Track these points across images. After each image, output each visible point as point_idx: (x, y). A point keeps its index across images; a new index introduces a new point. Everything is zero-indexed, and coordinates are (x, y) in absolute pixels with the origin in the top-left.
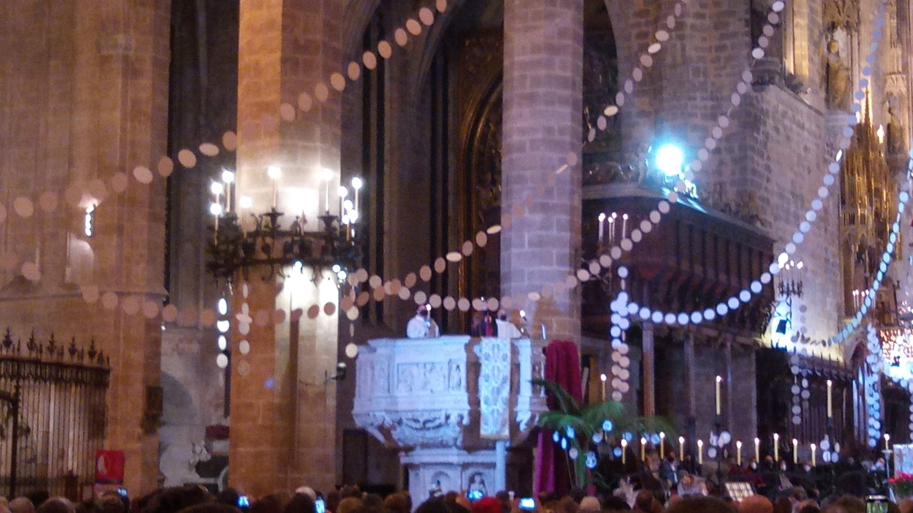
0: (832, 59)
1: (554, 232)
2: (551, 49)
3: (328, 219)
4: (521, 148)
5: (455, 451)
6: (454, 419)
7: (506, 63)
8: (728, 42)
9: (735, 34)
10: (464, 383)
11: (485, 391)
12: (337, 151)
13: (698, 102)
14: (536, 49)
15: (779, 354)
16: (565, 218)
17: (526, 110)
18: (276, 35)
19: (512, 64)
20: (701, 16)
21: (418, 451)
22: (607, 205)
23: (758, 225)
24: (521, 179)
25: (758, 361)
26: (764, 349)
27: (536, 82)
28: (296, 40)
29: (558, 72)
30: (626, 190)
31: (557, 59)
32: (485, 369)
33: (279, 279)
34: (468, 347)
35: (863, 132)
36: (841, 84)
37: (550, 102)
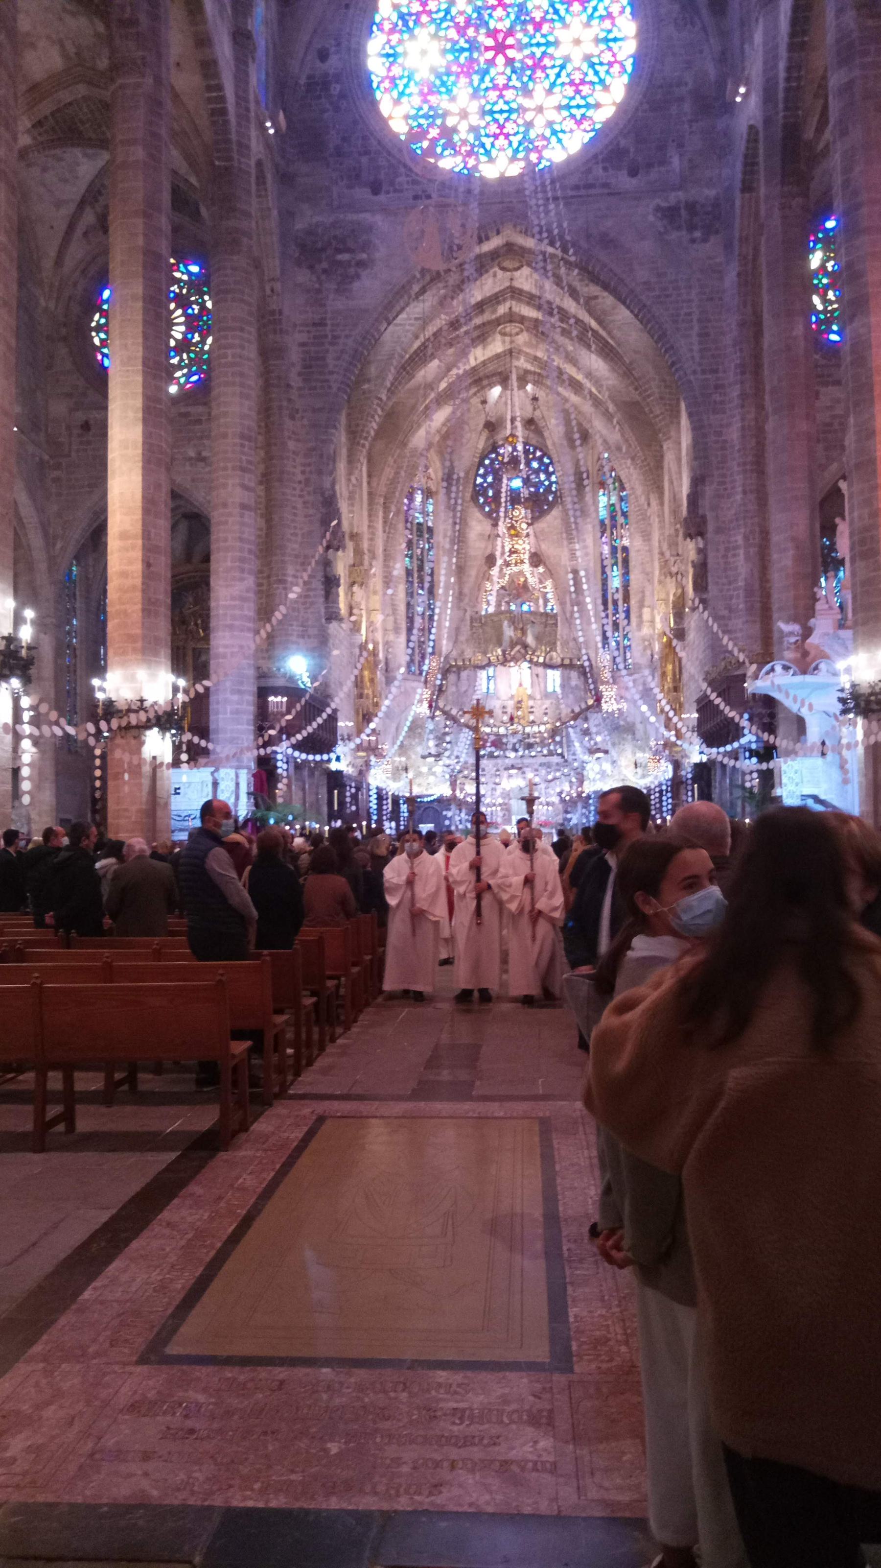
2: (243, 599)
7: (213, 604)
8: (311, 593)
9: (315, 589)
14: (233, 598)
15: (339, 773)
17: (227, 634)
18: (138, 595)
21: (176, 833)
22: (276, 691)
27: (234, 618)
28: (149, 599)
29: (246, 613)
30: (280, 683)
31: (246, 605)
33: (143, 738)
34: (212, 773)
35: (363, 647)
37: (242, 631)
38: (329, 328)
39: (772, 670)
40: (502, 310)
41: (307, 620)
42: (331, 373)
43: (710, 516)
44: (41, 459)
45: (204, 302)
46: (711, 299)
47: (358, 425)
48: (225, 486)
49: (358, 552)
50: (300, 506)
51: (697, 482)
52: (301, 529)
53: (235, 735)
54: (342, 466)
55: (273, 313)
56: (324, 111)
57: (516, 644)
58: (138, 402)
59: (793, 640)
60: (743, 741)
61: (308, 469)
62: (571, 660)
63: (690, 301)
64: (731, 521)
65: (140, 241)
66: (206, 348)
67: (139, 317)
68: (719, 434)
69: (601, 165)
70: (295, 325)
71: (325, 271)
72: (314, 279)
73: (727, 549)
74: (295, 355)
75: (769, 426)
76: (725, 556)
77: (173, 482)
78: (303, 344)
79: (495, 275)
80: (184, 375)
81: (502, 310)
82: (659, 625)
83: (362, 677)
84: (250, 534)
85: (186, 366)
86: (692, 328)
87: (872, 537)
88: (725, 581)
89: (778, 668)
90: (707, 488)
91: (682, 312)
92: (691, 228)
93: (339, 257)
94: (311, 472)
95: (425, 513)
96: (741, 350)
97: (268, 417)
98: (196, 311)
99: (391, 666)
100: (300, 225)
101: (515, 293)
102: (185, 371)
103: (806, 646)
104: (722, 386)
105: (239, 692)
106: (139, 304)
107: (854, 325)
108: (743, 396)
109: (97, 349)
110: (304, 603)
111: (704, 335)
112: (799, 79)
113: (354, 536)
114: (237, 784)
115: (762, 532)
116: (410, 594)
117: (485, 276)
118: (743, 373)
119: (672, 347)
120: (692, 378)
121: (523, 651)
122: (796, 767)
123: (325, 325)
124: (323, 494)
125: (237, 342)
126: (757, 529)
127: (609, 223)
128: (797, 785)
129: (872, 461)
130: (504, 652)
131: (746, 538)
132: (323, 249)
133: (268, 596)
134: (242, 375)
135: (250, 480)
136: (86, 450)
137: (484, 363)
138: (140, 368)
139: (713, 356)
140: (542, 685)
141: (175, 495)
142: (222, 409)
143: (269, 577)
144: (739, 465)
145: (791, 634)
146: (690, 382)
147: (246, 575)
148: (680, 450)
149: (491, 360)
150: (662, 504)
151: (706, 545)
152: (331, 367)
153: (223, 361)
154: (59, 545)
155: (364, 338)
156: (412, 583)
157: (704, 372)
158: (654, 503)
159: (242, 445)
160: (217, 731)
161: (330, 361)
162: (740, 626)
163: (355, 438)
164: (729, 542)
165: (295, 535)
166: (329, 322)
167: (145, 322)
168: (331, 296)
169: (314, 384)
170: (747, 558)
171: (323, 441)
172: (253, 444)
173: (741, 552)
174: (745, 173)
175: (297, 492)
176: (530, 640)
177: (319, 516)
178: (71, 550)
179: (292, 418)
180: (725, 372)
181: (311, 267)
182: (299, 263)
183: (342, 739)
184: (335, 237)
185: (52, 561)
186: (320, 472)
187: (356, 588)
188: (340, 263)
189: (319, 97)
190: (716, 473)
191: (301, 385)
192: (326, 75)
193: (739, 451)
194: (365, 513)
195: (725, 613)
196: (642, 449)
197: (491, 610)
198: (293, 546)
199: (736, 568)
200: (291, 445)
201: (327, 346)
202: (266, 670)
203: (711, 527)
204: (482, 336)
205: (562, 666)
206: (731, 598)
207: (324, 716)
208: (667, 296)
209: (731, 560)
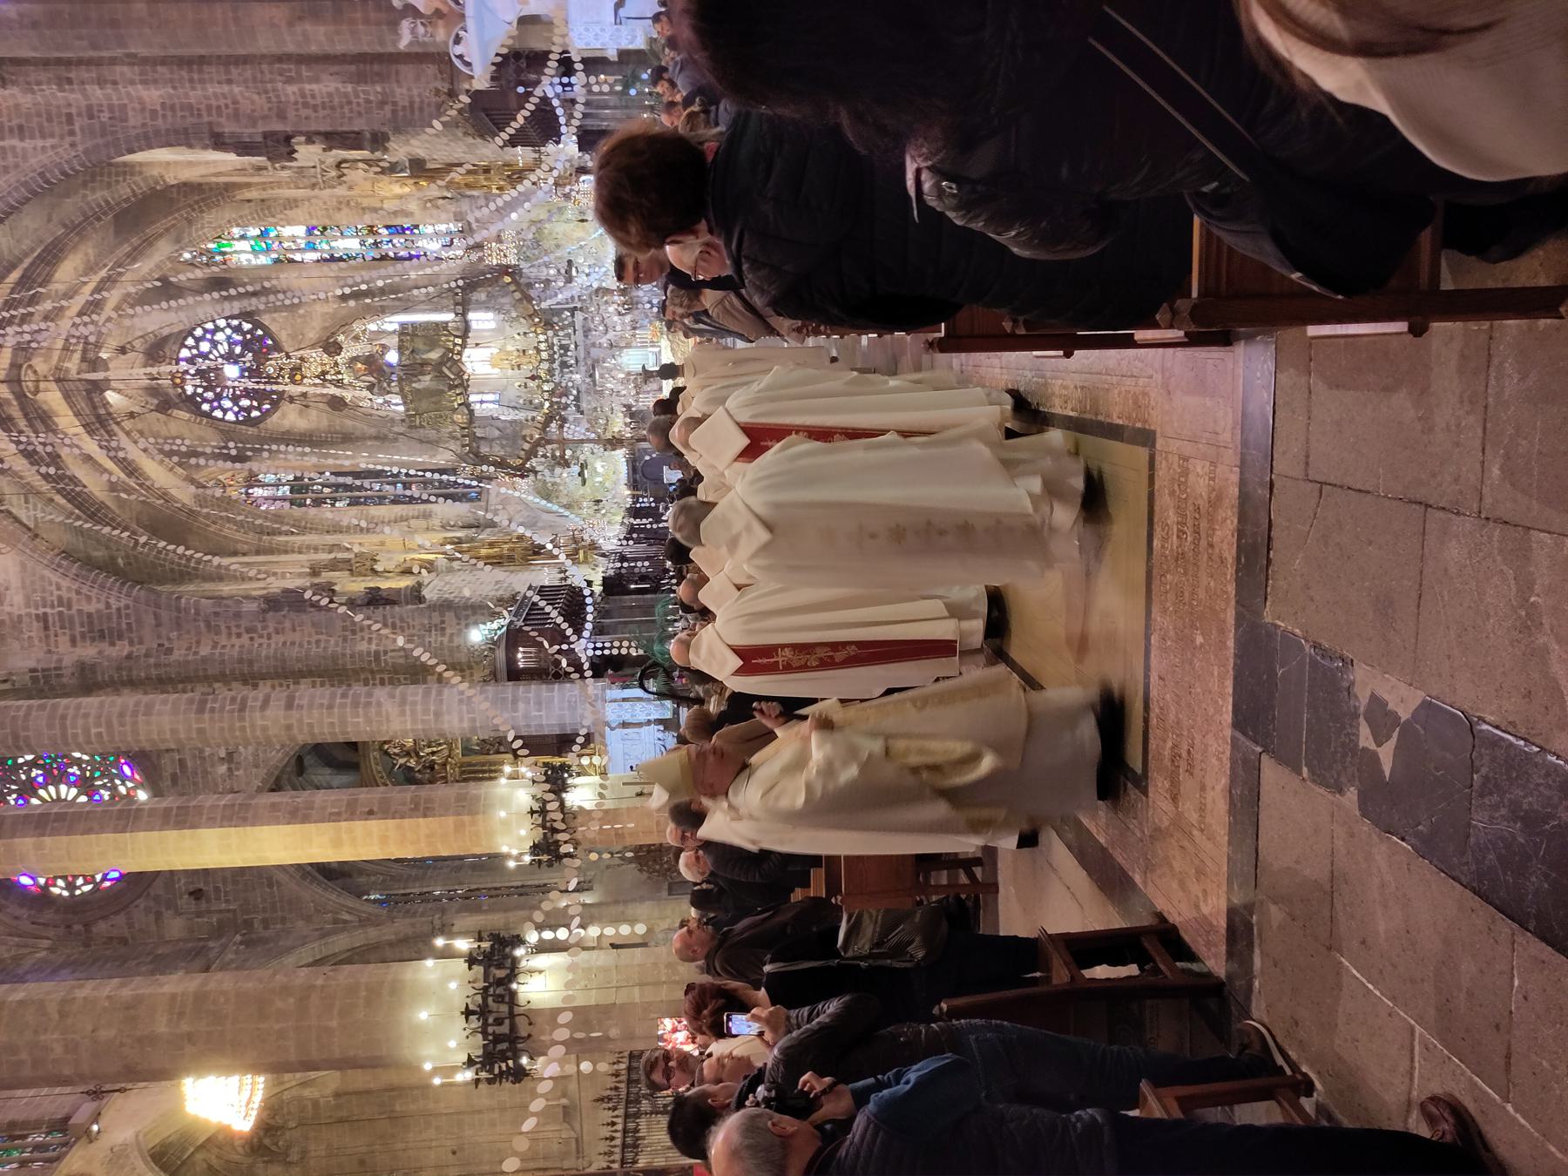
1: (531, 695)
2: (403, 702)
4: (473, 720)
6: (660, 735)
8: (390, 621)
9: (384, 616)
11: (642, 718)
13: (432, 640)
14: (403, 713)
16: (521, 689)
17: (446, 718)
18: (406, 821)
20: (370, 639)
22: (511, 661)
27: (426, 711)
28: (411, 809)
31: (410, 699)
32: (628, 718)
33: (575, 808)
34: (612, 729)
37: (441, 700)
38: (48, 610)
39: (460, 57)
41: (423, 625)
42: (108, 606)
43: (262, 128)
44: (241, 943)
45: (26, 763)
47: (172, 570)
48: (265, 729)
49: (334, 565)
50: (281, 638)
52: (310, 635)
53: (566, 704)
54: (226, 589)
55: (35, 680)
57: (441, 372)
58: (172, 835)
59: (421, 30)
61: (234, 630)
62: (457, 304)
66: (86, 757)
67: (64, 840)
68: (154, 113)
70: (50, 652)
73: (306, 105)
74: (88, 652)
75: (143, 52)
76: (315, 108)
77: (259, 790)
78: (73, 642)
80: (123, 783)
82: (407, 190)
83: (488, 557)
84: (323, 694)
85: (112, 781)
86: (13, 148)
88: (346, 109)
89: (458, 50)
90: (226, 130)
94: (238, 626)
95: (277, 485)
96: (39, 83)
97: (170, 680)
98: (40, 772)
99: (472, 521)
102: (118, 782)
103: (429, 13)
104: (89, 108)
105: (515, 701)
106: (47, 840)
108: (101, 82)
109: (97, 885)
110: (401, 627)
111: (21, 132)
113: (315, 572)
114: (624, 700)
116: (381, 500)
118: (70, 81)
120: (80, 148)
121: (449, 364)
122: (582, 29)
124: (264, 611)
125: (80, 722)
126: (277, 66)
130: (451, 387)
131: (289, 81)
133: (396, 673)
136: (226, 893)
137: (77, 414)
138: (128, 834)
140: (486, 334)
141: (276, 787)
142: (168, 736)
143: (372, 672)
144: (193, 89)
145: (413, 31)
147: (373, 700)
148: (176, 163)
149: (72, 406)
150: (248, 185)
151: (301, 133)
152: (101, 606)
153: (105, 738)
154: (346, 917)
156: (366, 498)
157: (72, 133)
158: (248, 195)
159: (212, 710)
160: (562, 726)
161: (92, 608)
162: (405, 91)
163: (189, 573)
164: (296, 103)
165: (318, 642)
166: (41, 611)
169: (124, 626)
170: (317, 80)
171: (197, 613)
173: (307, 87)
175: (265, 641)
176: (434, 355)
178: (351, 902)
179: (169, 651)
180: (70, 105)
183: (565, 579)
185: (365, 922)
186: (238, 615)
187: (379, 567)
190: (206, 119)
191: (126, 642)
193: (174, 88)
194: (283, 558)
195: (388, 108)
196: (178, 210)
197: (397, 399)
198: (333, 645)
199: (330, 95)
200: (205, 651)
201: (73, 611)
202: (487, 672)
203: (277, 126)
205: (464, 314)
206: (368, 101)
207: (536, 598)
209: (319, 101)
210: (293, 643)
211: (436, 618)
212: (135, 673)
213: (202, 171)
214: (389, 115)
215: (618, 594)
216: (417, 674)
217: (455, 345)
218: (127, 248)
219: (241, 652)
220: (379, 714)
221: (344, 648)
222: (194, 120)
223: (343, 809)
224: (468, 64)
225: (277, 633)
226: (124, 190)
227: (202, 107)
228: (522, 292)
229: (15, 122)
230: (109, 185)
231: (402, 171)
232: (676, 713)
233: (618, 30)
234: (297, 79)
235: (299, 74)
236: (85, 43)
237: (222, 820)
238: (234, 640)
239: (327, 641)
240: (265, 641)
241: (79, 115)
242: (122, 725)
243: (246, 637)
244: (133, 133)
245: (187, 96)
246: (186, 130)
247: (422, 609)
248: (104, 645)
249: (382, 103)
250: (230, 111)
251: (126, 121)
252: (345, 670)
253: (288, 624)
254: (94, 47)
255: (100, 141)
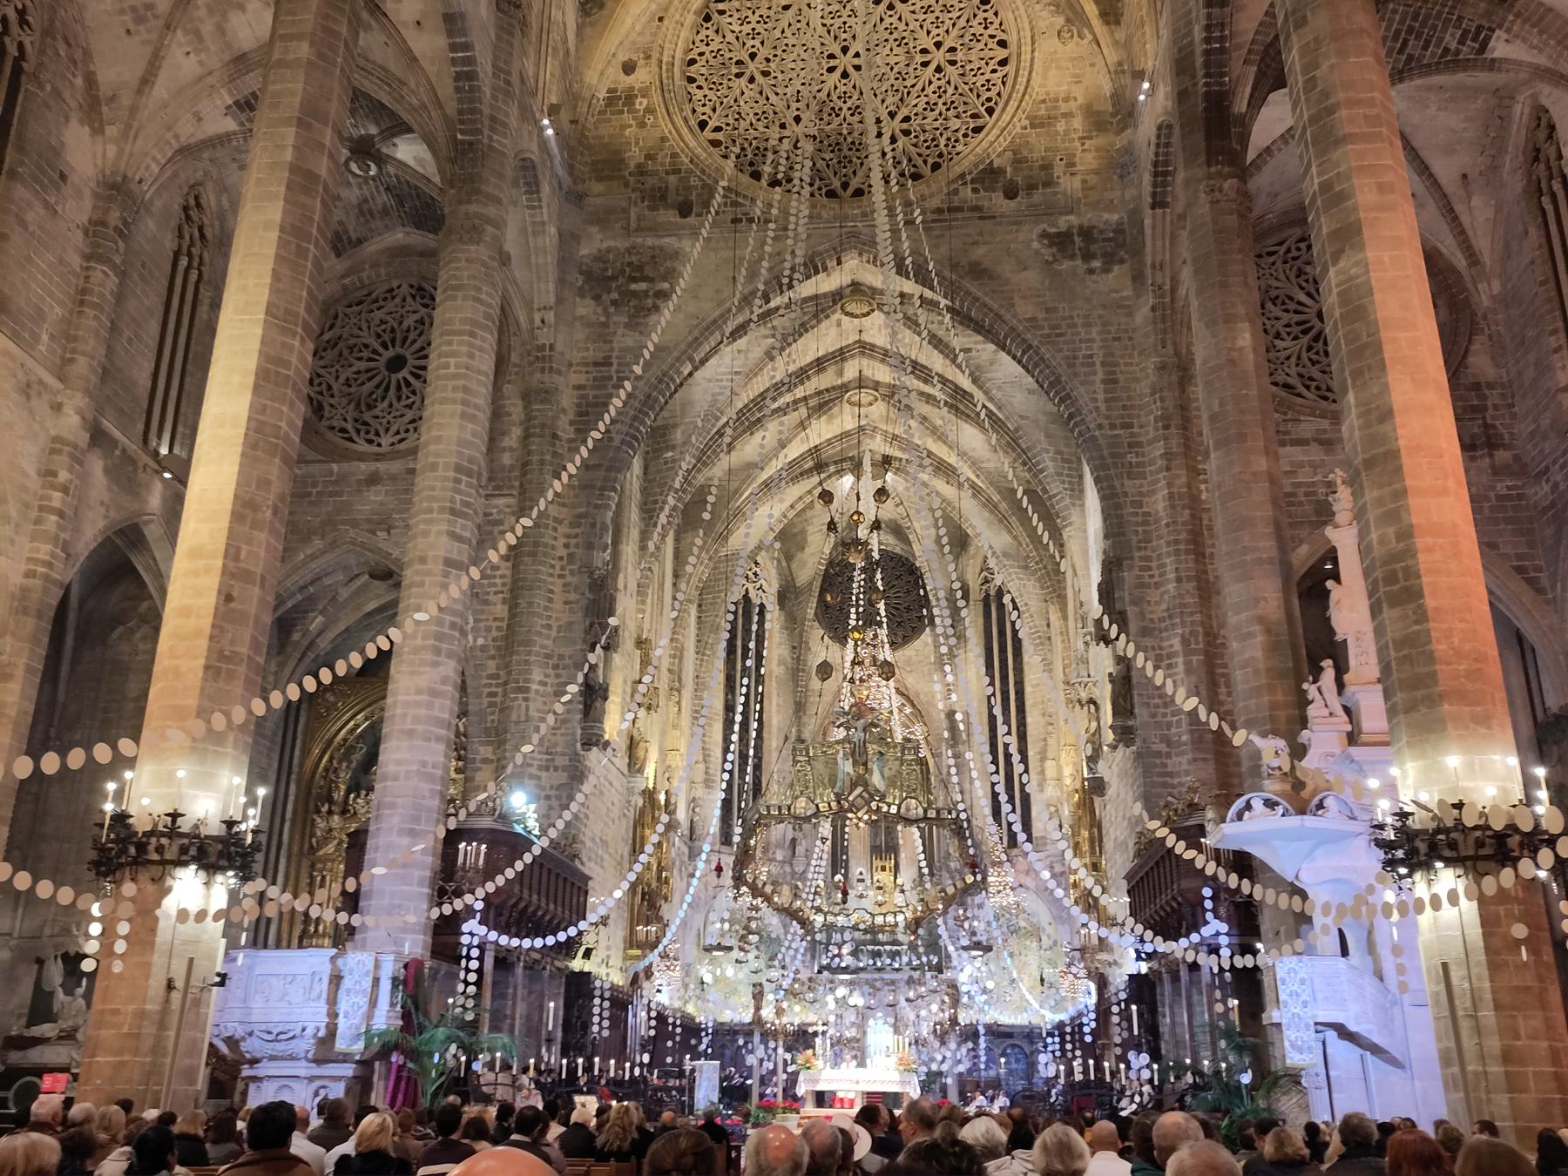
0: (636, 735)
3: (230, 824)
5: (304, 1063)
6: (309, 1032)
10: (324, 995)
11: (343, 1006)
12: (245, 760)
14: (419, 692)
15: (585, 977)
17: (405, 744)
18: (204, 643)
19: (395, 702)
20: (545, 684)
21: (264, 1063)
23: (577, 862)
24: (392, 806)
25: (568, 984)
26: (573, 973)
27: (416, 720)
28: (222, 651)
29: (436, 713)
31: (438, 702)
32: (347, 983)
33: (169, 882)
34: (333, 959)
35: (649, 795)
36: (641, 753)
37: (428, 739)
38: (614, 368)
39: (1248, 807)
40: (851, 371)
41: (555, 745)
46: (1119, 339)
47: (656, 502)
48: (425, 534)
50: (558, 589)
51: (1112, 566)
52: (558, 619)
53: (397, 902)
55: (542, 348)
56: (624, 127)
58: (251, 364)
60: (1207, 931)
61: (573, 541)
63: (1088, 341)
64: (1162, 620)
65: (288, 155)
67: (271, 251)
69: (969, 187)
70: (570, 365)
71: (614, 303)
72: (599, 310)
78: (579, 387)
79: (839, 324)
81: (851, 371)
82: (1068, 781)
87: (1406, 570)
88: (1157, 701)
89: (1257, 804)
91: (1080, 354)
92: (1088, 256)
93: (634, 287)
94: (577, 546)
96: (1162, 399)
97: (524, 474)
100: (585, 250)
101: (865, 348)
104: (1140, 444)
107: (1342, 264)
108: (1168, 456)
111: (1111, 382)
112: (1222, 39)
114: (376, 981)
115: (1206, 634)
117: (825, 324)
119: (1068, 396)
122: (1302, 974)
123: (611, 364)
125: (464, 349)
126: (1201, 630)
127: (980, 251)
128: (1305, 1004)
129: (1394, 455)
131: (1185, 642)
132: (614, 278)
133: (501, 711)
134: (466, 389)
135: (464, 527)
137: (829, 442)
138: (262, 316)
139: (1124, 407)
142: (435, 433)
143: (506, 683)
144: (1168, 544)
146: (1094, 438)
147: (442, 659)
148: (1086, 539)
150: (1065, 618)
155: (660, 381)
157: (1112, 427)
158: (1055, 617)
159: (457, 481)
162: (1185, 767)
163: (651, 518)
164: (1161, 648)
165: (549, 627)
166: (615, 361)
167: (279, 258)
168: (620, 331)
171: (597, 507)
172: (474, 481)
173: (1180, 660)
174: (1155, 185)
175: (557, 571)
176: (876, 780)
177: (584, 603)
181: (597, 298)
182: (581, 293)
184: (629, 264)
186: (590, 546)
188: (635, 294)
189: (622, 112)
190: (1137, 554)
192: (632, 88)
193: (1167, 525)
195: (1163, 747)
198: (544, 643)
204: (823, 404)
208: (1061, 335)
210: (550, 600)
211: (561, 761)
212: (537, 440)
213: (1079, 563)
214: (1155, 747)
215: (567, 991)
216: (497, 735)
217: (889, 805)
218: (996, 498)
219: (546, 545)
220: (423, 663)
221: (537, 654)
222: (1134, 544)
223: (243, 565)
224: (1240, 817)
225: (565, 585)
226: (1055, 488)
227: (1149, 553)
228: (954, 896)
229: (1121, 377)
230: (1058, 474)
231: (1090, 769)
232: (345, 1058)
233: (1307, 1027)
234: (1188, 652)
235: (1194, 652)
236: (1216, 408)
237: (258, 421)
238: (562, 541)
239: (548, 637)
240: (557, 571)
241: (1132, 435)
242: (454, 389)
243: (563, 552)
244: (1117, 483)
245: (1160, 537)
246: (1123, 534)
247: (574, 745)
248: (571, 416)
249: (1169, 743)
250: (1147, 580)
251: (1129, 478)
252: (512, 654)
253: (573, 597)
254: (1213, 418)
255: (1105, 453)
